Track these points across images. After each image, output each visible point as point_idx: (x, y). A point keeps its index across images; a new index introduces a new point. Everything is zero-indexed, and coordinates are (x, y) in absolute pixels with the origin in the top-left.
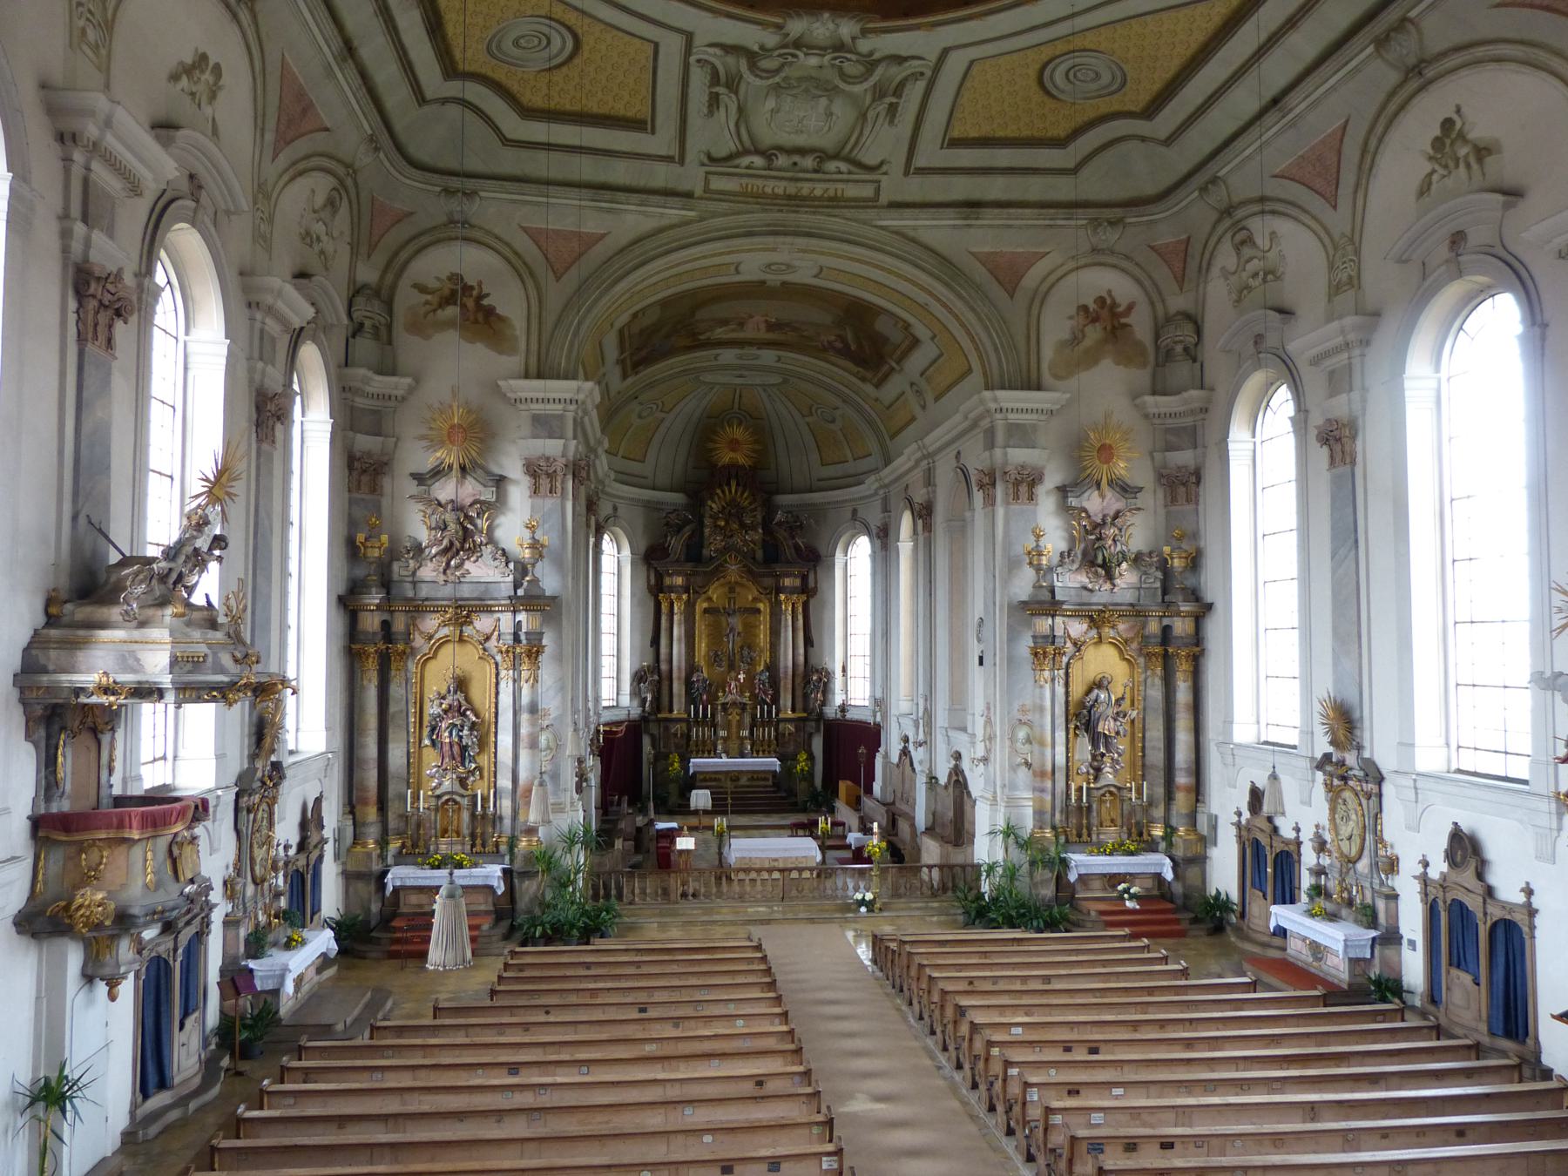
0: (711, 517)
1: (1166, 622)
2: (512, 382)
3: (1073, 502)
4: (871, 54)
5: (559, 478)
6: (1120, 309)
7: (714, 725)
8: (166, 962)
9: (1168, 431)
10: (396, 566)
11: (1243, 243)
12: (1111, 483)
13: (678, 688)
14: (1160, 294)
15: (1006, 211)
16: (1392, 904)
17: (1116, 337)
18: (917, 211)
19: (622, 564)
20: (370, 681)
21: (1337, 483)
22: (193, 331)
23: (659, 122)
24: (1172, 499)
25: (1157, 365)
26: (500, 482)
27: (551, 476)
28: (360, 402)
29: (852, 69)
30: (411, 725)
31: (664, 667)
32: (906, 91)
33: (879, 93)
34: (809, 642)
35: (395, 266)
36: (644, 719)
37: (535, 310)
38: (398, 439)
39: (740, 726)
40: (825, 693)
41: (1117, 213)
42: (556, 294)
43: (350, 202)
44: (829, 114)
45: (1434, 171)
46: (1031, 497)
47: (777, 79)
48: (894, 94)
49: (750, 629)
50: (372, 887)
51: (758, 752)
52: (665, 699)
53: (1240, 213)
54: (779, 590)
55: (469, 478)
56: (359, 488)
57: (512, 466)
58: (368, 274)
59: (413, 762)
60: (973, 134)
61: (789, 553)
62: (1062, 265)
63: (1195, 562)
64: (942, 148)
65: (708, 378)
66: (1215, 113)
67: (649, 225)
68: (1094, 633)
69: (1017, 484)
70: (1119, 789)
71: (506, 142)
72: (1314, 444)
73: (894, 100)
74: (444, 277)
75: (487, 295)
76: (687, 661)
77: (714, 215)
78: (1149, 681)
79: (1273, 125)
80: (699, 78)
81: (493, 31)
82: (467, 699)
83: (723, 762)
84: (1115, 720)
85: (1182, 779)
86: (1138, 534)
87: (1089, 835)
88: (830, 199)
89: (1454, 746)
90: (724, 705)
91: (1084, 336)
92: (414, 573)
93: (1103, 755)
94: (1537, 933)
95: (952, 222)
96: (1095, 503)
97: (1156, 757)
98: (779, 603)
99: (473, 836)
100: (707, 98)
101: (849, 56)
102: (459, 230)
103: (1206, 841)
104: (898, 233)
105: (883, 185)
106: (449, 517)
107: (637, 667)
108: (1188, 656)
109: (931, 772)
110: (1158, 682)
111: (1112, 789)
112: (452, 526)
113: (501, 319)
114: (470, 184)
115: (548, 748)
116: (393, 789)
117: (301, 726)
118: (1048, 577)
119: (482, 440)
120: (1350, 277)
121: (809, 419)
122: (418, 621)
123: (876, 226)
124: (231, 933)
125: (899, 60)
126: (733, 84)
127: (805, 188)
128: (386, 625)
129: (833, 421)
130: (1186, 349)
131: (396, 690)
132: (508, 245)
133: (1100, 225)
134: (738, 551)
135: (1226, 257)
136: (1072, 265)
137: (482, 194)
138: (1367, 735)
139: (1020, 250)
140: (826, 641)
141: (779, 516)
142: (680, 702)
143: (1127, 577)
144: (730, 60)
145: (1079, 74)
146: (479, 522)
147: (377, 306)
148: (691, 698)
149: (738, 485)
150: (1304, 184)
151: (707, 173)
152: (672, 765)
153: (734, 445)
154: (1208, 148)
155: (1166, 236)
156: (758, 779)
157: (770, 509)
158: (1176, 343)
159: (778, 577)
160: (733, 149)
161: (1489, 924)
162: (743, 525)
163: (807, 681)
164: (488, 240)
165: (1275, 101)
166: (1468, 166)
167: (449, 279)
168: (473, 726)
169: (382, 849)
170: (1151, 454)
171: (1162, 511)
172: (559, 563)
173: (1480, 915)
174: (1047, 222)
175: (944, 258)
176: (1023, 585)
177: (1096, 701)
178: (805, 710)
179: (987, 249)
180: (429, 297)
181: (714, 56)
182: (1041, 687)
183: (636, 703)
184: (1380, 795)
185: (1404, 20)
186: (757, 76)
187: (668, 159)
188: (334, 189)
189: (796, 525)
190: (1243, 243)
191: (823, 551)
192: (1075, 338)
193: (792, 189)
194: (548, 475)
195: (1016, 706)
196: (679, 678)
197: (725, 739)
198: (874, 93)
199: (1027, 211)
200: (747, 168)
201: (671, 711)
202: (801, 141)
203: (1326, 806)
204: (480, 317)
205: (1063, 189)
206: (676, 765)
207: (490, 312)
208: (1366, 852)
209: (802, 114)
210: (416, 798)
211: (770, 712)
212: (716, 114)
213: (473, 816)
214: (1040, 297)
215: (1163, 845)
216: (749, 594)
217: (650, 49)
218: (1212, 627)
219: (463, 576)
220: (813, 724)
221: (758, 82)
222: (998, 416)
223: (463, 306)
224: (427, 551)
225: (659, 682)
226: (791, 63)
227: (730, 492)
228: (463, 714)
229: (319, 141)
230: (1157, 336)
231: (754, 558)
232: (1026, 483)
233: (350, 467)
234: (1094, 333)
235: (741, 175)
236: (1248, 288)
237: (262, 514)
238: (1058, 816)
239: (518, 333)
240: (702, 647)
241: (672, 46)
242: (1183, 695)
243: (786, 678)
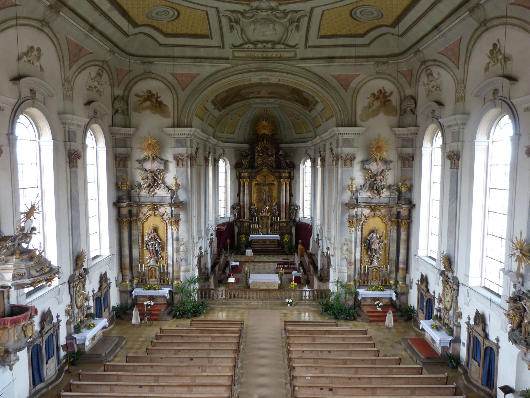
0: (257, 152)
1: (399, 210)
2: (168, 129)
3: (366, 167)
4: (285, 10)
5: (185, 161)
6: (387, 94)
7: (258, 224)
8: (40, 345)
9: (403, 140)
10: (132, 192)
11: (429, 74)
12: (380, 160)
13: (246, 211)
14: (403, 88)
15: (343, 60)
16: (458, 329)
17: (385, 104)
18: (311, 61)
19: (227, 169)
20: (125, 230)
21: (452, 173)
22: (41, 137)
23: (213, 35)
24: (404, 165)
25: (401, 115)
26: (166, 162)
27: (183, 160)
28: (118, 137)
29: (281, 15)
30: (140, 243)
31: (242, 204)
32: (301, 21)
33: (291, 22)
34: (291, 195)
35: (128, 88)
36: (235, 221)
37: (176, 102)
38: (132, 148)
39: (267, 224)
41: (386, 59)
42: (183, 95)
43: (107, 72)
44: (274, 29)
45: (490, 63)
46: (351, 165)
47: (253, 19)
48: (297, 22)
49: (271, 190)
50: (128, 295)
51: (273, 232)
52: (242, 214)
53: (428, 64)
54: (281, 177)
55: (155, 161)
56: (119, 166)
57: (169, 157)
58: (118, 92)
59: (141, 255)
60: (329, 34)
61: (284, 165)
62: (366, 78)
63: (410, 189)
64: (317, 39)
65: (254, 106)
66: (416, 28)
67: (215, 70)
68: (372, 213)
69: (346, 161)
70: (379, 268)
71: (161, 45)
72: (446, 159)
73: (297, 24)
74: (145, 90)
75: (160, 97)
76: (249, 201)
77: (237, 65)
78: (392, 230)
79: (436, 35)
80: (224, 21)
81: (147, 12)
82: (158, 235)
83: (261, 236)
84: (379, 244)
85: (401, 266)
86: (390, 178)
87: (368, 283)
88: (279, 58)
89: (483, 278)
90: (261, 217)
91: (373, 105)
92: (139, 194)
93: (374, 256)
94: (500, 355)
95: (324, 64)
96: (374, 167)
97: (393, 257)
98: (280, 182)
99: (160, 279)
100: (229, 27)
101: (277, 11)
102: (148, 75)
103: (408, 287)
104: (304, 69)
105: (298, 52)
106: (149, 175)
108: (405, 223)
109: (322, 250)
110: (395, 231)
111: (376, 268)
112: (150, 178)
113: (165, 105)
114: (151, 60)
115: (184, 251)
116: (134, 263)
117: (101, 247)
118: (356, 194)
119: (159, 149)
120: (462, 96)
121: (291, 118)
122: (141, 209)
123: (296, 67)
124: (69, 326)
125: (296, 12)
126: (237, 22)
127: (269, 54)
128: (130, 211)
129: (299, 119)
130: (411, 110)
131: (135, 232)
132: (166, 79)
133: (379, 64)
134: (267, 163)
135: (424, 79)
136: (369, 78)
137: (155, 63)
138: (455, 268)
139: (350, 73)
141: (280, 152)
142: (247, 216)
143: (385, 193)
144: (234, 15)
145: (365, 13)
146: (159, 176)
147: (123, 103)
148: (251, 214)
149: (266, 141)
150: (448, 57)
151: (233, 51)
152: (242, 238)
153: (264, 128)
154: (422, 34)
155: (404, 67)
156: (272, 242)
157: (278, 149)
158: (408, 107)
159: (281, 173)
160: (242, 43)
161: (485, 347)
162: (268, 155)
163: (290, 209)
164: (159, 78)
165: (436, 27)
166: (501, 63)
167: (147, 92)
168: (159, 243)
169: (131, 283)
170: (397, 148)
171: (400, 169)
172: (186, 190)
173: (482, 344)
174: (359, 63)
175: (322, 78)
176: (347, 197)
177: (372, 237)
178: (290, 218)
179: (337, 73)
180: (140, 99)
181: (228, 14)
182: (351, 233)
183: (232, 216)
184: (458, 290)
185: (478, 4)
186: (245, 19)
187: (219, 47)
188: (99, 70)
189: (286, 155)
190: (429, 74)
191: (296, 164)
192: (370, 106)
193: (264, 55)
194: (182, 160)
195: (343, 238)
196: (247, 208)
197: (262, 228)
198: (290, 22)
199: (352, 59)
200: (248, 48)
201: (244, 218)
202: (266, 38)
203: (442, 288)
204: (158, 105)
205: (365, 52)
206: (244, 238)
207: (160, 103)
208: (452, 308)
209: (264, 30)
210: (142, 267)
211: (277, 219)
212: (233, 32)
213: (160, 272)
214: (357, 91)
215: (394, 287)
216: (270, 179)
217: (205, 13)
218: (414, 213)
219: (155, 194)
220: (292, 223)
221: (246, 20)
222: (340, 136)
223: (152, 101)
224: (143, 186)
225: (240, 208)
226: (257, 14)
227: (264, 143)
228: (156, 240)
229: (90, 57)
230: (401, 105)
231: (272, 167)
232: (350, 160)
233: (116, 159)
234: (377, 104)
235: (246, 51)
236: (431, 91)
237: (73, 191)
238: (357, 276)
239: (170, 110)
240: (255, 197)
241: (212, 13)
242: (403, 236)
243: (283, 208)
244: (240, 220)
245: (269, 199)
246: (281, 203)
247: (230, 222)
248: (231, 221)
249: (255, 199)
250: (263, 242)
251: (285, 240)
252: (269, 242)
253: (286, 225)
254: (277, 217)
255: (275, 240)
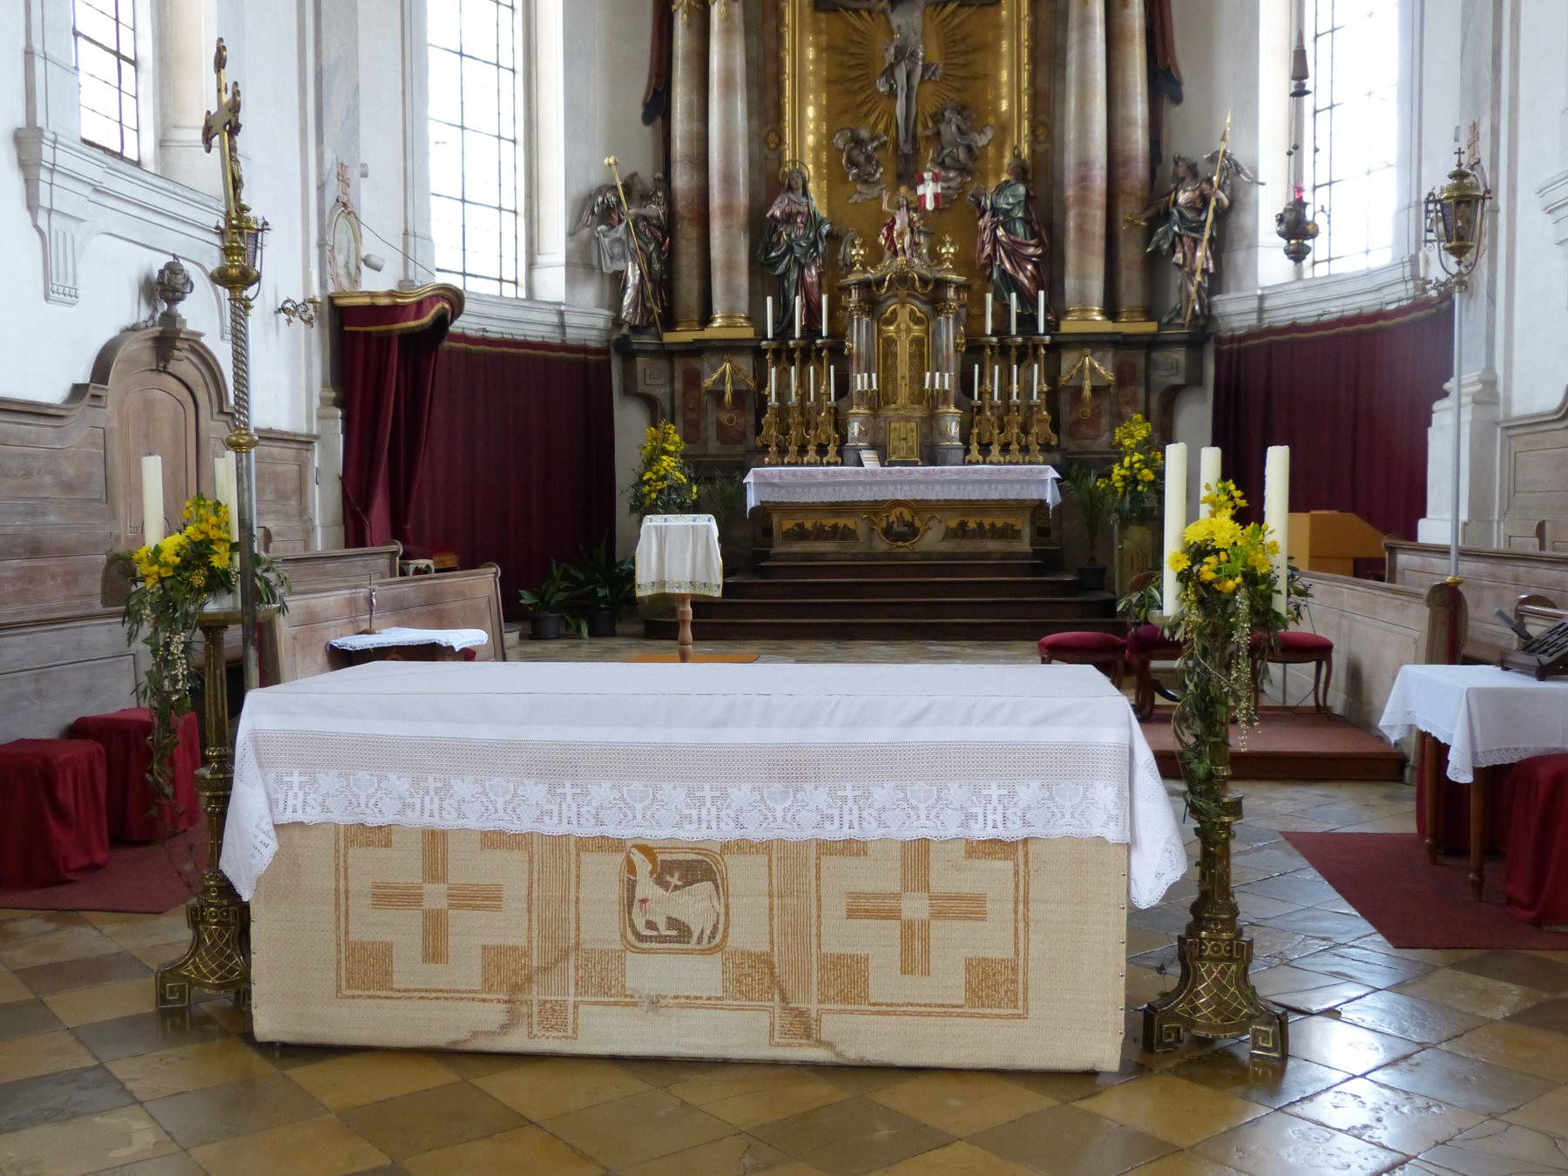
7: (837, 351)
31: (682, 180)
36: (621, 345)
40: (1219, 247)
51: (985, 449)
76: (753, 164)
107: (596, 179)
140: (1226, 65)
142: (730, 289)
156: (980, 533)
163: (1158, 212)
178: (1149, 313)
183: (589, 294)
196: (728, 210)
197: (878, 402)
201: (706, 319)
211: (1027, 321)
220: (1179, 356)
225: (669, 227)
243: (1083, 200)
244: (669, 337)
245: (949, 130)
246: (1070, 159)
247: (564, 347)
248: (572, 335)
249: (810, 140)
250: (888, 532)
251: (1118, 472)
252: (950, 534)
253: (1124, 375)
254: (1028, 300)
255: (1002, 506)
